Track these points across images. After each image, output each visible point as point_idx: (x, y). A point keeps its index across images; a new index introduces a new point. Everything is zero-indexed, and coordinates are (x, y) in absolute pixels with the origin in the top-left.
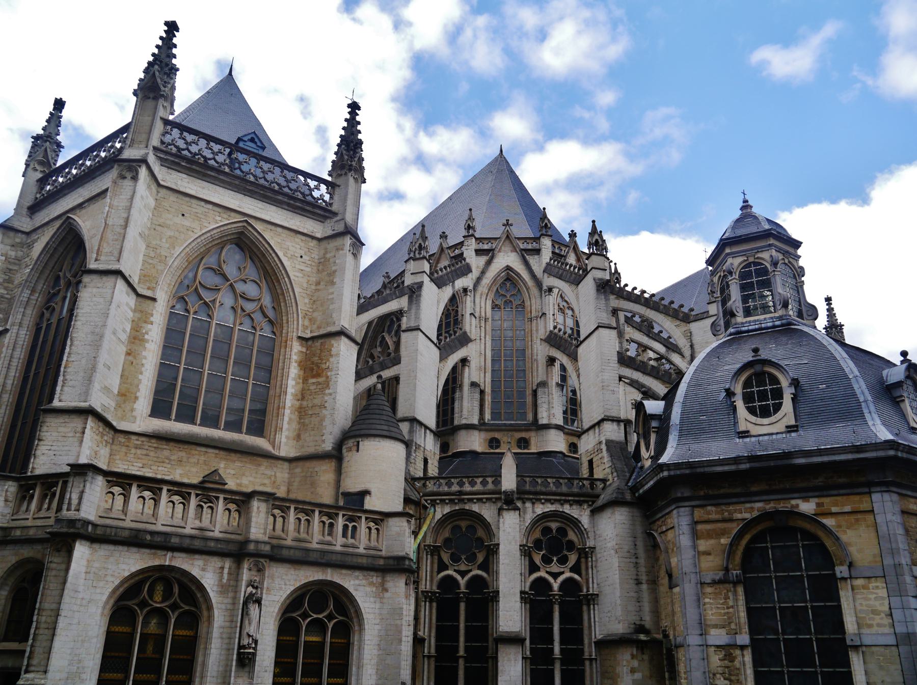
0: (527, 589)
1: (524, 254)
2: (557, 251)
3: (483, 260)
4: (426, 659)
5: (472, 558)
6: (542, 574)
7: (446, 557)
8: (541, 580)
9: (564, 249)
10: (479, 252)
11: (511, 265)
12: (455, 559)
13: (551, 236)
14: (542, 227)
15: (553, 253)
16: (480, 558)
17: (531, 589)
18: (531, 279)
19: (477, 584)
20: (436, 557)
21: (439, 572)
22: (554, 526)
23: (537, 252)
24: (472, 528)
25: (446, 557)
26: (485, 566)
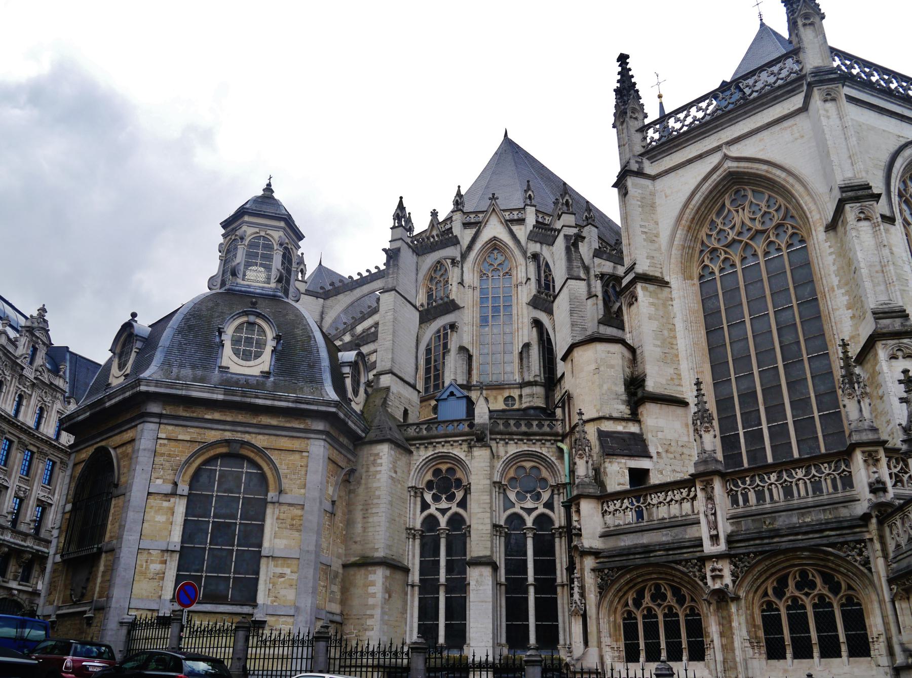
0: (502, 523)
1: (508, 223)
2: (540, 220)
3: (469, 233)
4: (409, 587)
5: (451, 498)
6: (517, 509)
7: (428, 497)
8: (515, 516)
9: (547, 218)
10: (466, 225)
11: (497, 235)
12: (436, 498)
13: (535, 206)
14: (526, 198)
15: (537, 222)
16: (459, 495)
17: (505, 523)
18: (515, 244)
19: (457, 522)
20: (419, 499)
21: (422, 511)
22: (528, 465)
23: (521, 221)
24: (451, 470)
25: (428, 497)
26: (463, 504)
